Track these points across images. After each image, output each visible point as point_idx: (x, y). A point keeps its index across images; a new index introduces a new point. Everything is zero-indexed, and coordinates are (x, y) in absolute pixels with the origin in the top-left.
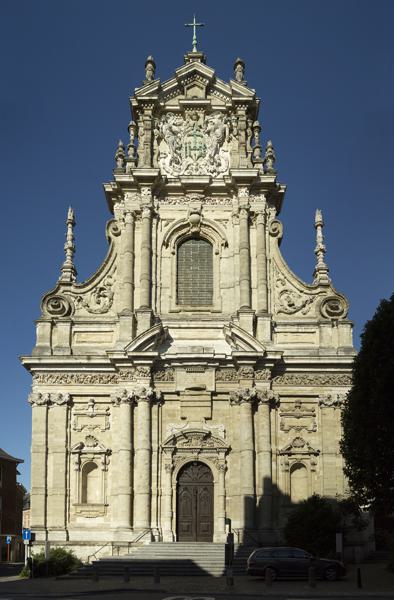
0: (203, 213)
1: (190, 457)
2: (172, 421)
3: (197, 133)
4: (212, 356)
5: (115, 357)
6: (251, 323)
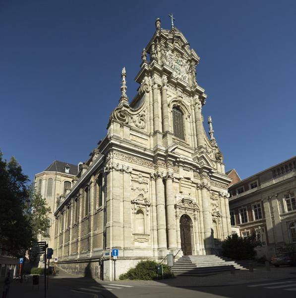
1: (183, 212)
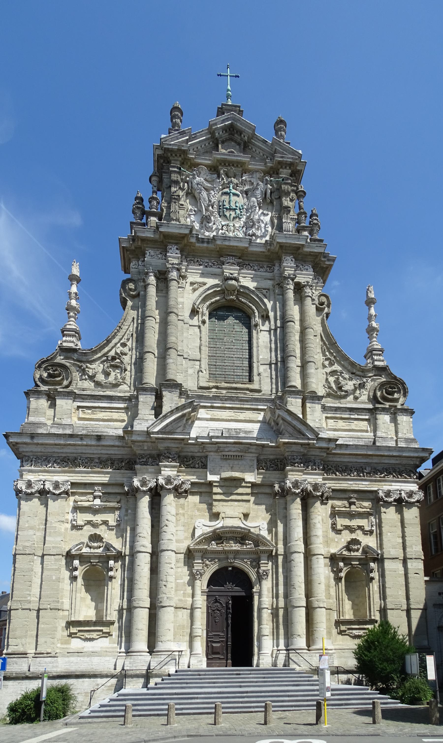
0: (241, 279)
3: (234, 191)
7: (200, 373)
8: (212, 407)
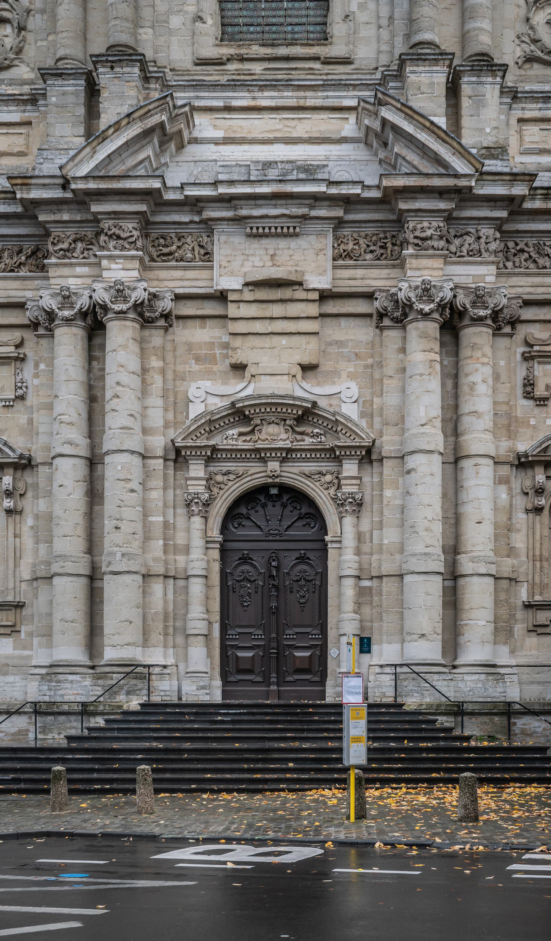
2: (208, 375)
4: (322, 188)
5: (35, 194)
6: (441, 90)
7: (199, 24)
8: (228, 109)
